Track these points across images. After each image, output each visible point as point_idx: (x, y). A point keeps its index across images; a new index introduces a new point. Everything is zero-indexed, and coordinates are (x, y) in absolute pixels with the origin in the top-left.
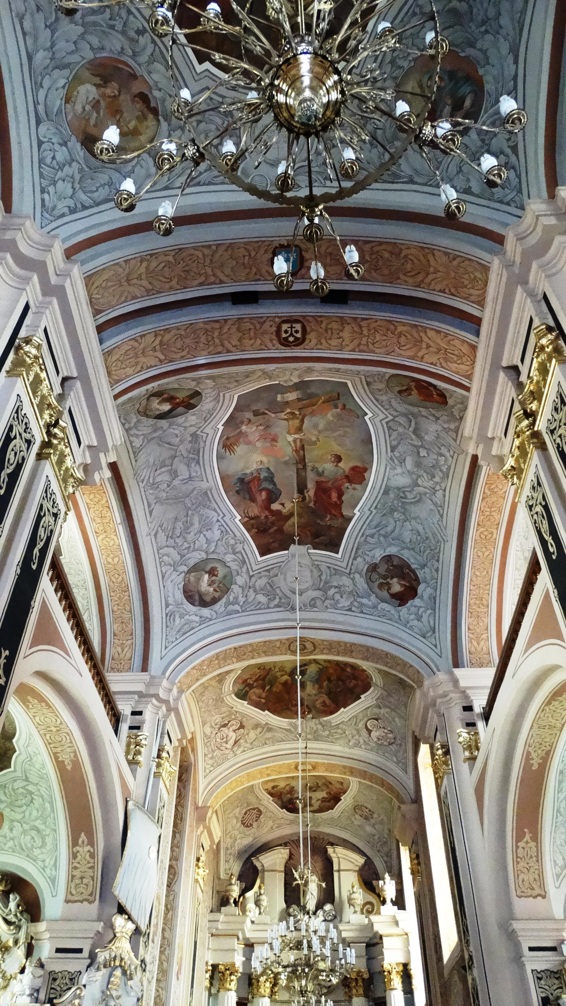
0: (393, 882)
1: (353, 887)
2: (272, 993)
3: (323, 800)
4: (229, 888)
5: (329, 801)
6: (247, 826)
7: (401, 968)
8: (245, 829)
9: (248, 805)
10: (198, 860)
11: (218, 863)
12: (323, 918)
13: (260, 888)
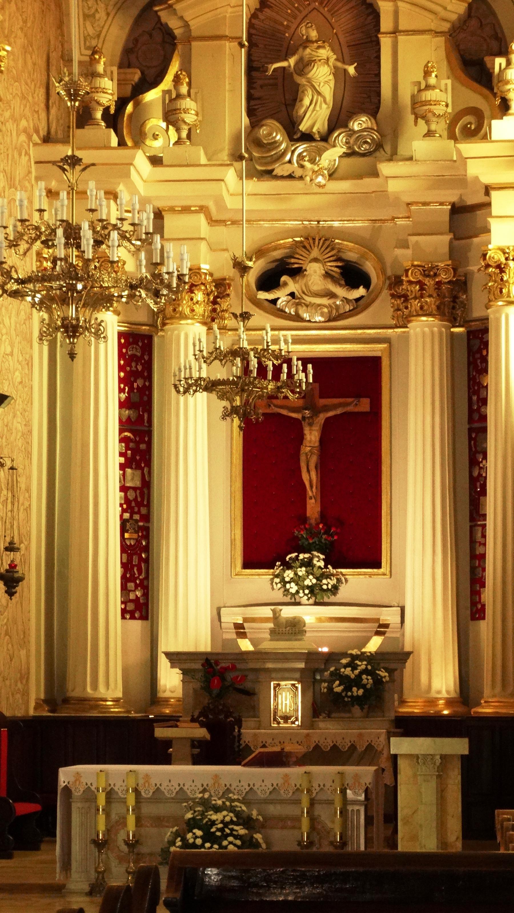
1: (427, 73)
11: (61, 24)
12: (344, 150)
13: (177, 80)
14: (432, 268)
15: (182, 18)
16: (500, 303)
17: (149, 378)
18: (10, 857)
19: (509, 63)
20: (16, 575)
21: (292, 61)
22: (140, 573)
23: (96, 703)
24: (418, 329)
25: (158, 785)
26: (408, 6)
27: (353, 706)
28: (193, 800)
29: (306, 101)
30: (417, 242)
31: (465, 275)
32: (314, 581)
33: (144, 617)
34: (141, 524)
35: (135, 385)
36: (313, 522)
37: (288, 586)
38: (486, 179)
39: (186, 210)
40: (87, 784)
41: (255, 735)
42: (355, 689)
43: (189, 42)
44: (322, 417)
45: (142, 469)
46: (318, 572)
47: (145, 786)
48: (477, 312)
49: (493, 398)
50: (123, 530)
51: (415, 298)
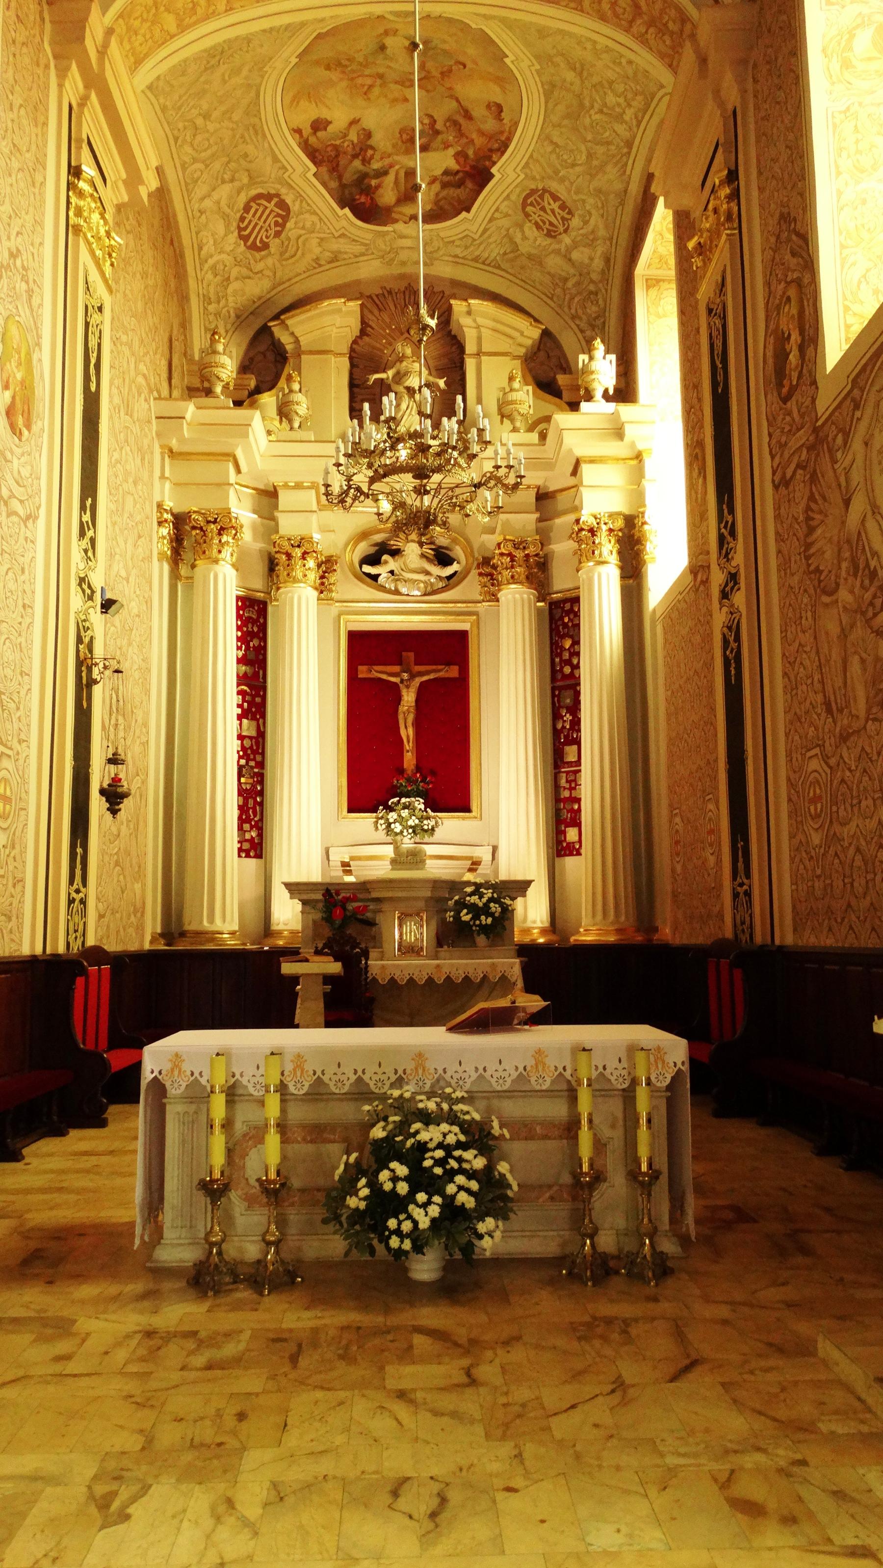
0: (613, 357)
1: (511, 379)
2: (322, 587)
3: (449, 180)
4: (207, 359)
5: (460, 184)
6: (254, 247)
7: (620, 523)
10: (75, 172)
11: (185, 325)
14: (521, 542)
15: (292, 334)
16: (591, 564)
17: (264, 639)
18: (102, 1123)
19: (591, 358)
20: (120, 790)
21: (391, 373)
22: (255, 816)
23: (211, 936)
24: (510, 596)
25: (319, 1073)
26: (490, 332)
27: (479, 935)
28: (383, 1098)
30: (507, 520)
31: (546, 556)
32: (417, 821)
33: (259, 856)
34: (256, 770)
35: (251, 644)
36: (409, 772)
37: (393, 826)
38: (579, 452)
39: (298, 486)
40: (192, 1074)
41: (383, 966)
42: (483, 917)
43: (299, 355)
44: (418, 681)
45: (258, 720)
46: (419, 814)
47: (295, 1073)
48: (560, 583)
49: (587, 650)
50: (240, 775)
51: (507, 568)
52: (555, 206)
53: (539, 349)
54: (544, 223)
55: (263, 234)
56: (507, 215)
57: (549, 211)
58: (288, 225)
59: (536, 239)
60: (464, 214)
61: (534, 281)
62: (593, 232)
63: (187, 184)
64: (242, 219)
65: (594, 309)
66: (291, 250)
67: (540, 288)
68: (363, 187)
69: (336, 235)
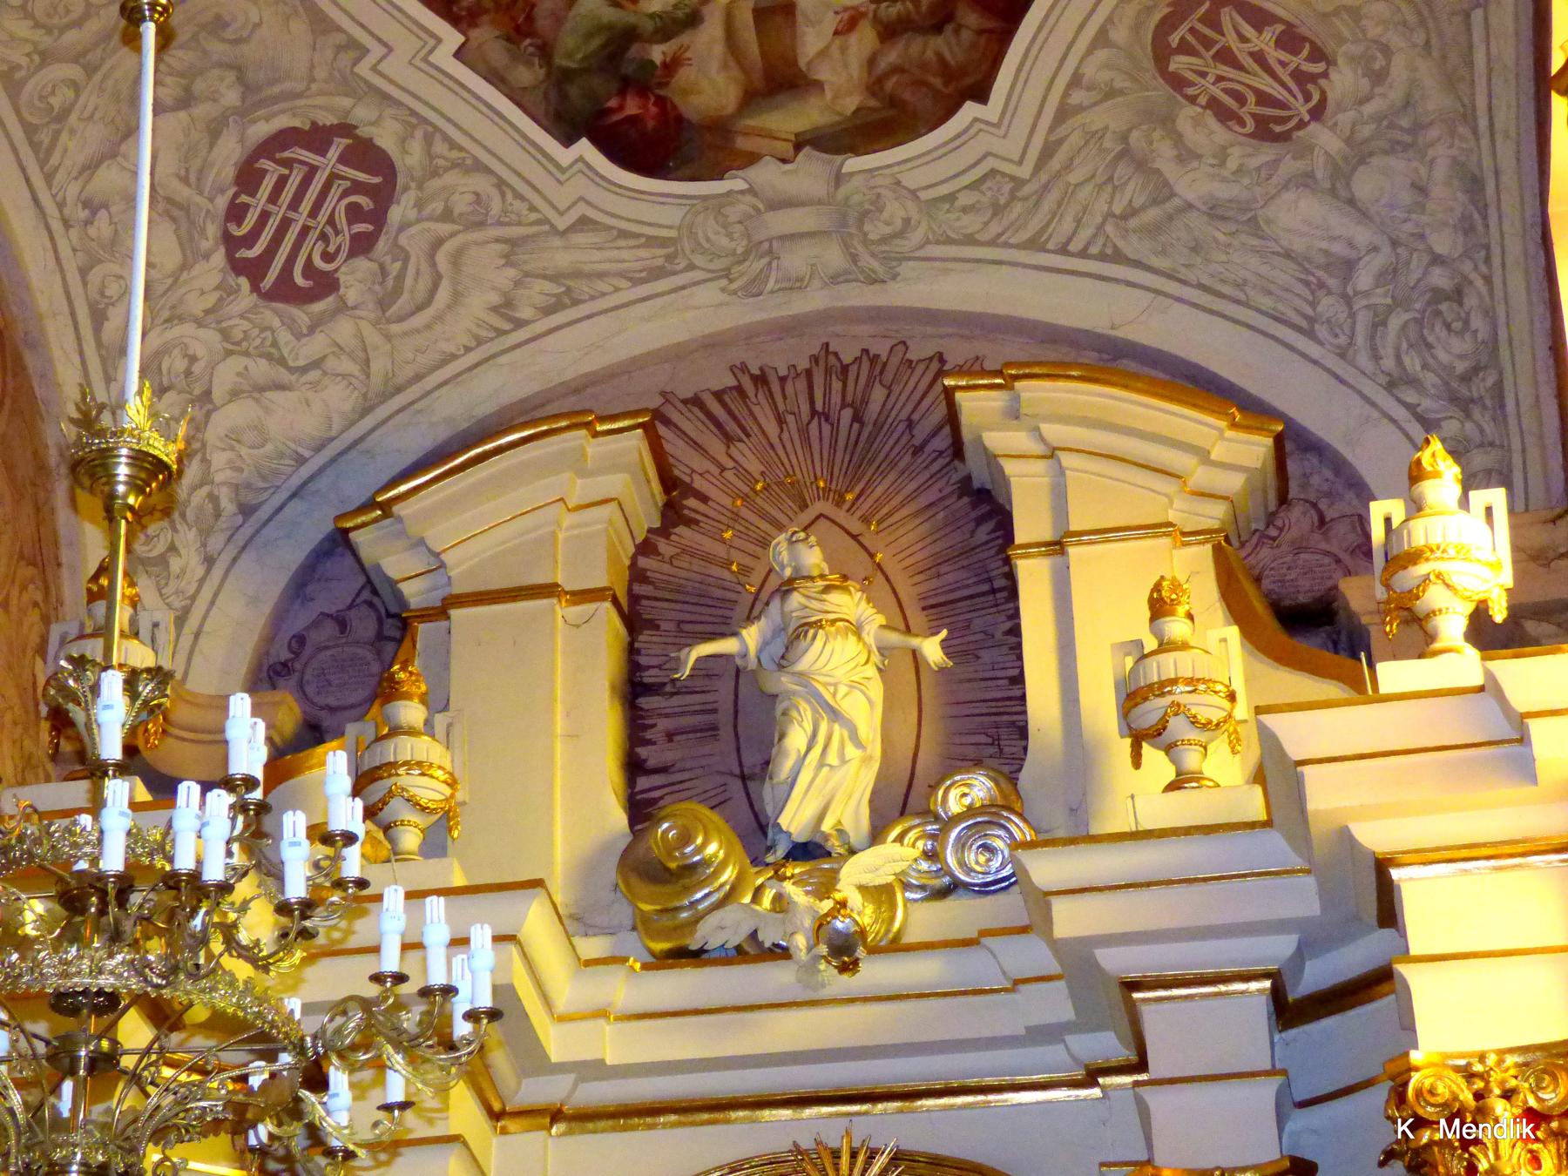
6: (284, 291)
8: (270, 315)
9: (254, 97)
19: (1416, 507)
21: (752, 636)
29: (796, 739)
52: (1265, 40)
53: (1283, 499)
54: (1241, 99)
55: (313, 249)
56: (1111, 93)
57: (1248, 62)
58: (395, 214)
59: (1222, 156)
60: (970, 109)
61: (1241, 285)
62: (1407, 103)
63: (30, 130)
64: (236, 213)
65: (1462, 345)
66: (415, 286)
67: (1266, 303)
68: (628, 69)
69: (562, 224)
